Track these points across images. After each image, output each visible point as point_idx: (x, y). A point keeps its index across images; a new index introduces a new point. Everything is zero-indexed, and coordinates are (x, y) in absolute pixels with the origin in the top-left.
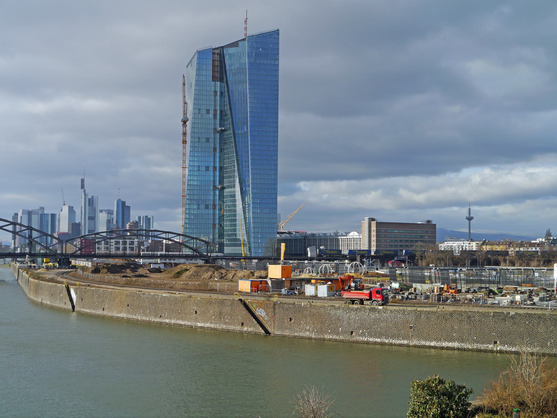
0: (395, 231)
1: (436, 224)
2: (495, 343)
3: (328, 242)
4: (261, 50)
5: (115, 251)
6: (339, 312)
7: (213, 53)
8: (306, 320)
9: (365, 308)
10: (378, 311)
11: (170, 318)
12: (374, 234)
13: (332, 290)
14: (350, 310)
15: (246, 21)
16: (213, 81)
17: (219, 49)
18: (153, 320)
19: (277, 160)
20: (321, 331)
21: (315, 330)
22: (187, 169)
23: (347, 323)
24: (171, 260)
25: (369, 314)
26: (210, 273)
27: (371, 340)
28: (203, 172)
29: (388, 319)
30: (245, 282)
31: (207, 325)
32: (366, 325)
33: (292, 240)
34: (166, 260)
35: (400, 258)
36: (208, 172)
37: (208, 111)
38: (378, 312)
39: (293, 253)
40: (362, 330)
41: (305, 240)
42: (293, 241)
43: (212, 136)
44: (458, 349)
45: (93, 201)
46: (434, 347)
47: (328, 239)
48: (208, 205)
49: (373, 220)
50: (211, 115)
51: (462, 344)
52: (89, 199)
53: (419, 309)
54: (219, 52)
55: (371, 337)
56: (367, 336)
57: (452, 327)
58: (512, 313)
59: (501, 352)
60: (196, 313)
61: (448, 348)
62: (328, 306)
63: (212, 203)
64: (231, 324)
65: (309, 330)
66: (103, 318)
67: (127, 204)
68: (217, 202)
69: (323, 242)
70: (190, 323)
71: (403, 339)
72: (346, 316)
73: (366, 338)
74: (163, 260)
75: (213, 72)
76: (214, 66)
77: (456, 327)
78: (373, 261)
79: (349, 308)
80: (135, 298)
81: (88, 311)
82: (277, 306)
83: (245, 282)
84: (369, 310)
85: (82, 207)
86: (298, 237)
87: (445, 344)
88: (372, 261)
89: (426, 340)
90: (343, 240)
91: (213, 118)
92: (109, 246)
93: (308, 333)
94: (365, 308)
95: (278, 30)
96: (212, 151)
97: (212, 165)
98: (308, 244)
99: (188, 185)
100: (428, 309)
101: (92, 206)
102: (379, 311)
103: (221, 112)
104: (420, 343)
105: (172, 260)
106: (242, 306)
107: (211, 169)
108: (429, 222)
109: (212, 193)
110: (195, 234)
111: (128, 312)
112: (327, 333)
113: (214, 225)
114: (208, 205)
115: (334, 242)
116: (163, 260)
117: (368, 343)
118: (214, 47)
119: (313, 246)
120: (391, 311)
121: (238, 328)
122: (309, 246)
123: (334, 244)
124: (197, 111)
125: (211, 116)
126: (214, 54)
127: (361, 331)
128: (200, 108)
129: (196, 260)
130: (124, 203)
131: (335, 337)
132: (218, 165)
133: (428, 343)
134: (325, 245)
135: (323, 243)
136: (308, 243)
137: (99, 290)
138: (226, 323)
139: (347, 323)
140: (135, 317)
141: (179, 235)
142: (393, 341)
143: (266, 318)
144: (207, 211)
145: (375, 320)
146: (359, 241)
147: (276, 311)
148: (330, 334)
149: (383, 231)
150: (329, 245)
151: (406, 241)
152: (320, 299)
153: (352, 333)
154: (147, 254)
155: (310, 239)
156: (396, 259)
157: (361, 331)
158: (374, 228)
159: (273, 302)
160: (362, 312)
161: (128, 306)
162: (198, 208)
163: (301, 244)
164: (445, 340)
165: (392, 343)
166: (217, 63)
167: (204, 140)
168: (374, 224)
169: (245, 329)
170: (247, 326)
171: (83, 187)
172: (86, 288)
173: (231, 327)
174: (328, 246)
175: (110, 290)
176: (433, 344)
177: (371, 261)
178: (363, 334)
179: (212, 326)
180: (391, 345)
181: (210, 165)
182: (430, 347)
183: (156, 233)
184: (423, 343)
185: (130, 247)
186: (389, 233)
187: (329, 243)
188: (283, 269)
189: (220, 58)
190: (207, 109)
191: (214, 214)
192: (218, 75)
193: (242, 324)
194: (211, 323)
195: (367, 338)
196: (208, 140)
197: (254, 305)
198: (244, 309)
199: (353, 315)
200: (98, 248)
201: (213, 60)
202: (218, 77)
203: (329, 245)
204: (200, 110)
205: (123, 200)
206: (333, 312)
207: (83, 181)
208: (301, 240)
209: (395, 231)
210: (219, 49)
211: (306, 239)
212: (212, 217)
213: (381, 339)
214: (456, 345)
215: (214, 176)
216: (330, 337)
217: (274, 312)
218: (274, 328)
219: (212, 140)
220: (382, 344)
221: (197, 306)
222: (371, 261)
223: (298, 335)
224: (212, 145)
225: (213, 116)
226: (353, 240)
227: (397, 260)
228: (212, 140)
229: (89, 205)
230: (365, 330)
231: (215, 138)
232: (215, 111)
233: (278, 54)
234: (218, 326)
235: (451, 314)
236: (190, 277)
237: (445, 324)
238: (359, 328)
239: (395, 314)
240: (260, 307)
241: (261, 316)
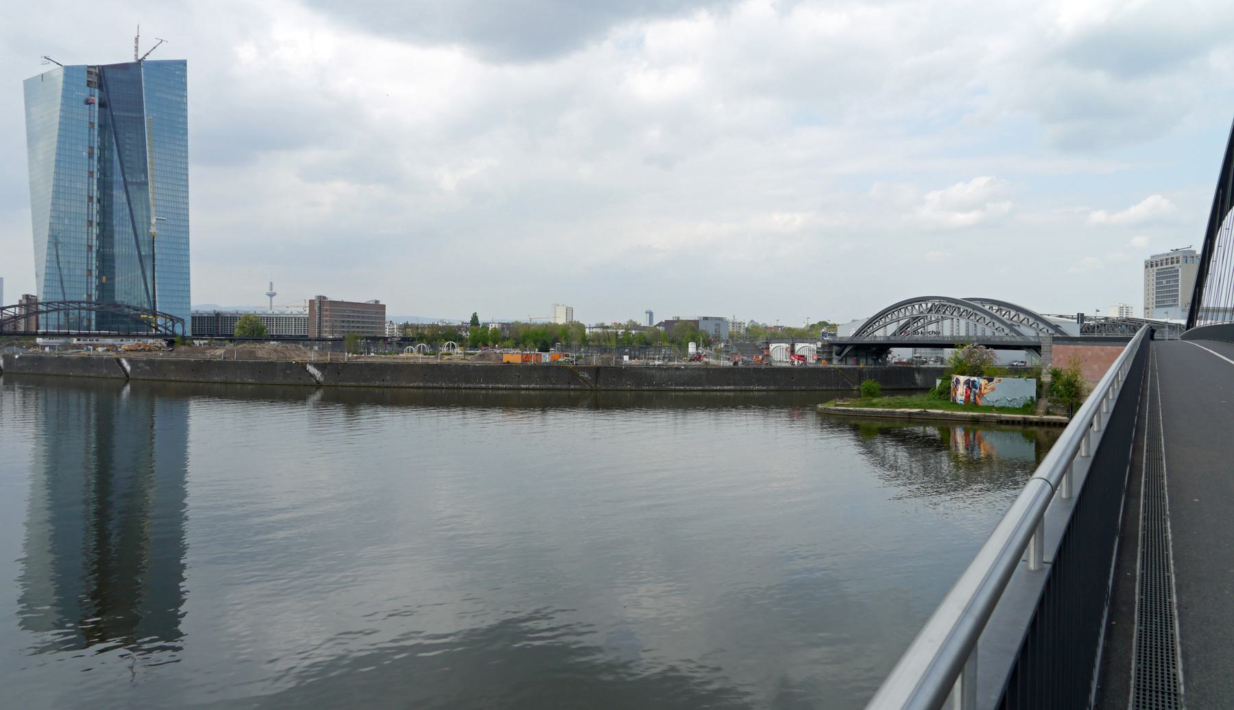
11: (488, 383)
34: (79, 340)
39: (197, 333)
41: (218, 317)
117: (675, 390)
131: (650, 387)
133: (715, 388)
138: (551, 383)
178: (672, 385)
180: (691, 390)
182: (716, 390)
193: (569, 383)
206: (648, 372)
214: (732, 387)
240: (583, 371)
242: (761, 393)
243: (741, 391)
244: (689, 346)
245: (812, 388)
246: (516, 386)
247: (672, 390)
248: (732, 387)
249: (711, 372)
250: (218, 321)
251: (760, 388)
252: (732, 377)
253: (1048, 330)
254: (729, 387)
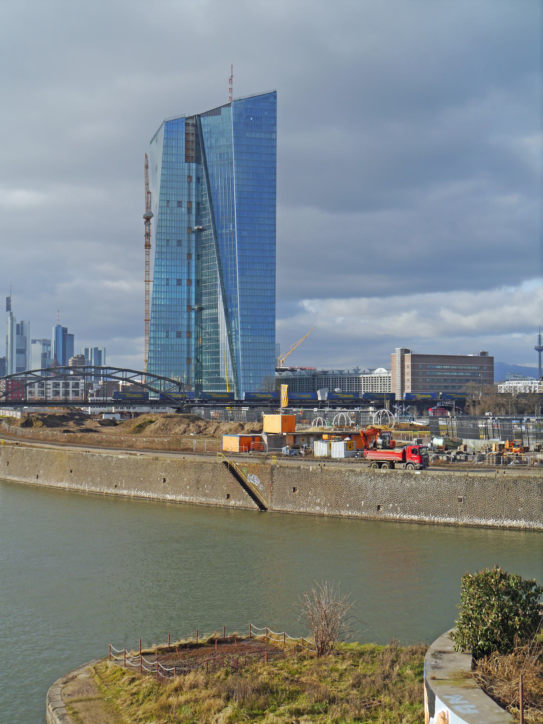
0: (437, 367)
1: (493, 358)
3: (345, 383)
4: (251, 119)
5: (53, 396)
7: (186, 123)
8: (315, 490)
9: (396, 473)
10: (414, 477)
11: (129, 489)
12: (408, 371)
13: (350, 449)
14: (376, 476)
15: (231, 80)
16: (186, 162)
17: (194, 118)
18: (105, 491)
19: (275, 270)
20: (337, 505)
21: (328, 505)
22: (151, 284)
23: (372, 494)
24: (129, 408)
25: (402, 482)
26: (183, 427)
27: (405, 517)
28: (173, 287)
29: (429, 488)
30: (231, 439)
31: (180, 498)
32: (398, 497)
33: (297, 380)
34: (122, 408)
35: (444, 404)
36: (180, 287)
37: (180, 204)
38: (415, 479)
40: (393, 504)
41: (314, 379)
42: (298, 381)
43: (185, 237)
44: (526, 530)
45: (22, 327)
47: (345, 378)
48: (180, 333)
49: (407, 351)
50: (183, 209)
51: (531, 523)
52: (18, 326)
53: (471, 474)
54: (194, 122)
55: (405, 513)
56: (400, 512)
57: (517, 499)
60: (165, 481)
61: (511, 529)
62: (346, 471)
63: (185, 329)
64: (213, 497)
65: (319, 504)
66: (37, 488)
67: (69, 332)
68: (193, 328)
69: (339, 382)
70: (156, 496)
71: (449, 516)
72: (371, 485)
73: (399, 515)
74: (119, 408)
75: (187, 149)
76: (187, 141)
77: (521, 499)
78: (407, 408)
79: (374, 474)
80: (81, 461)
81: (16, 479)
82: (275, 472)
83: (231, 439)
84: (402, 476)
85: (7, 336)
86: (303, 375)
87: (507, 523)
88: (405, 408)
89: (481, 517)
90: (366, 379)
91: (186, 213)
92: (44, 389)
93: (318, 508)
94: (396, 473)
95: (275, 92)
96: (186, 258)
97: (186, 277)
98: (318, 385)
99: (153, 305)
100: (483, 475)
101: (22, 334)
102: (416, 478)
103: (198, 204)
104: (472, 522)
105: (131, 408)
106: (227, 472)
107: (184, 282)
108: (483, 353)
109: (185, 316)
110: (162, 373)
111: (72, 480)
112: (343, 507)
113: (189, 359)
114: (180, 333)
115: (353, 383)
116: (119, 408)
118: (187, 116)
119: (325, 387)
120: (433, 478)
121: (223, 501)
122: (320, 387)
123: (353, 385)
124: (164, 204)
125: (184, 210)
126: (187, 125)
127: (391, 505)
128: (168, 199)
129: (164, 408)
130: (65, 330)
132: (193, 277)
133: (483, 522)
134: (341, 386)
135: (339, 384)
136: (318, 383)
137: (31, 450)
138: (206, 495)
139: (372, 494)
140: (81, 487)
141: (140, 373)
142: (436, 518)
143: (260, 488)
144: (179, 341)
145: (410, 490)
146: (388, 381)
147: (275, 478)
148: (348, 509)
149: (420, 367)
150: (346, 386)
151: (452, 380)
152: (335, 460)
153: (379, 507)
154: (97, 400)
155: (320, 379)
156: (438, 405)
157: (391, 505)
158: (408, 362)
159: (270, 466)
160: (392, 479)
161: (71, 472)
162: (167, 337)
163: (309, 386)
164: (507, 517)
165: (434, 522)
166: (192, 138)
167: (175, 243)
168: (408, 357)
169: (232, 503)
170: (235, 499)
171: (8, 308)
172: (13, 448)
173: (213, 501)
174: (345, 387)
175: (46, 450)
176: (490, 522)
177: (404, 408)
179: (187, 499)
180: (433, 524)
181: (183, 278)
183: (109, 372)
184: (477, 521)
185: (73, 391)
186: (429, 369)
187: (346, 384)
188: (284, 420)
189: (196, 130)
190: (178, 200)
191: (189, 345)
192: (193, 154)
193: (228, 496)
194: (185, 495)
195: (400, 515)
196: (179, 243)
197: (244, 471)
198: (231, 475)
200: (30, 392)
201: (187, 134)
202: (193, 157)
203: (346, 386)
204: (168, 202)
205: (64, 326)
206: (352, 479)
207: (8, 300)
208: (309, 379)
209: (437, 367)
210: (194, 118)
211: (316, 378)
212: (185, 349)
213: (418, 516)
214: (522, 523)
215: (189, 292)
216: (348, 513)
217: (271, 479)
218: (272, 502)
219: (185, 244)
220: (421, 523)
221: (166, 471)
222: (404, 408)
223: (305, 510)
224: (185, 251)
225: (186, 210)
226: (379, 380)
227: (441, 407)
228: (185, 244)
229: (18, 333)
230: (396, 504)
231: (189, 241)
232: (190, 203)
233: (275, 125)
234: (194, 499)
235: (515, 481)
236: (156, 432)
237: (507, 495)
238: (389, 501)
239: (438, 481)
241: (253, 485)
246: (160, 496)
250: (314, 382)
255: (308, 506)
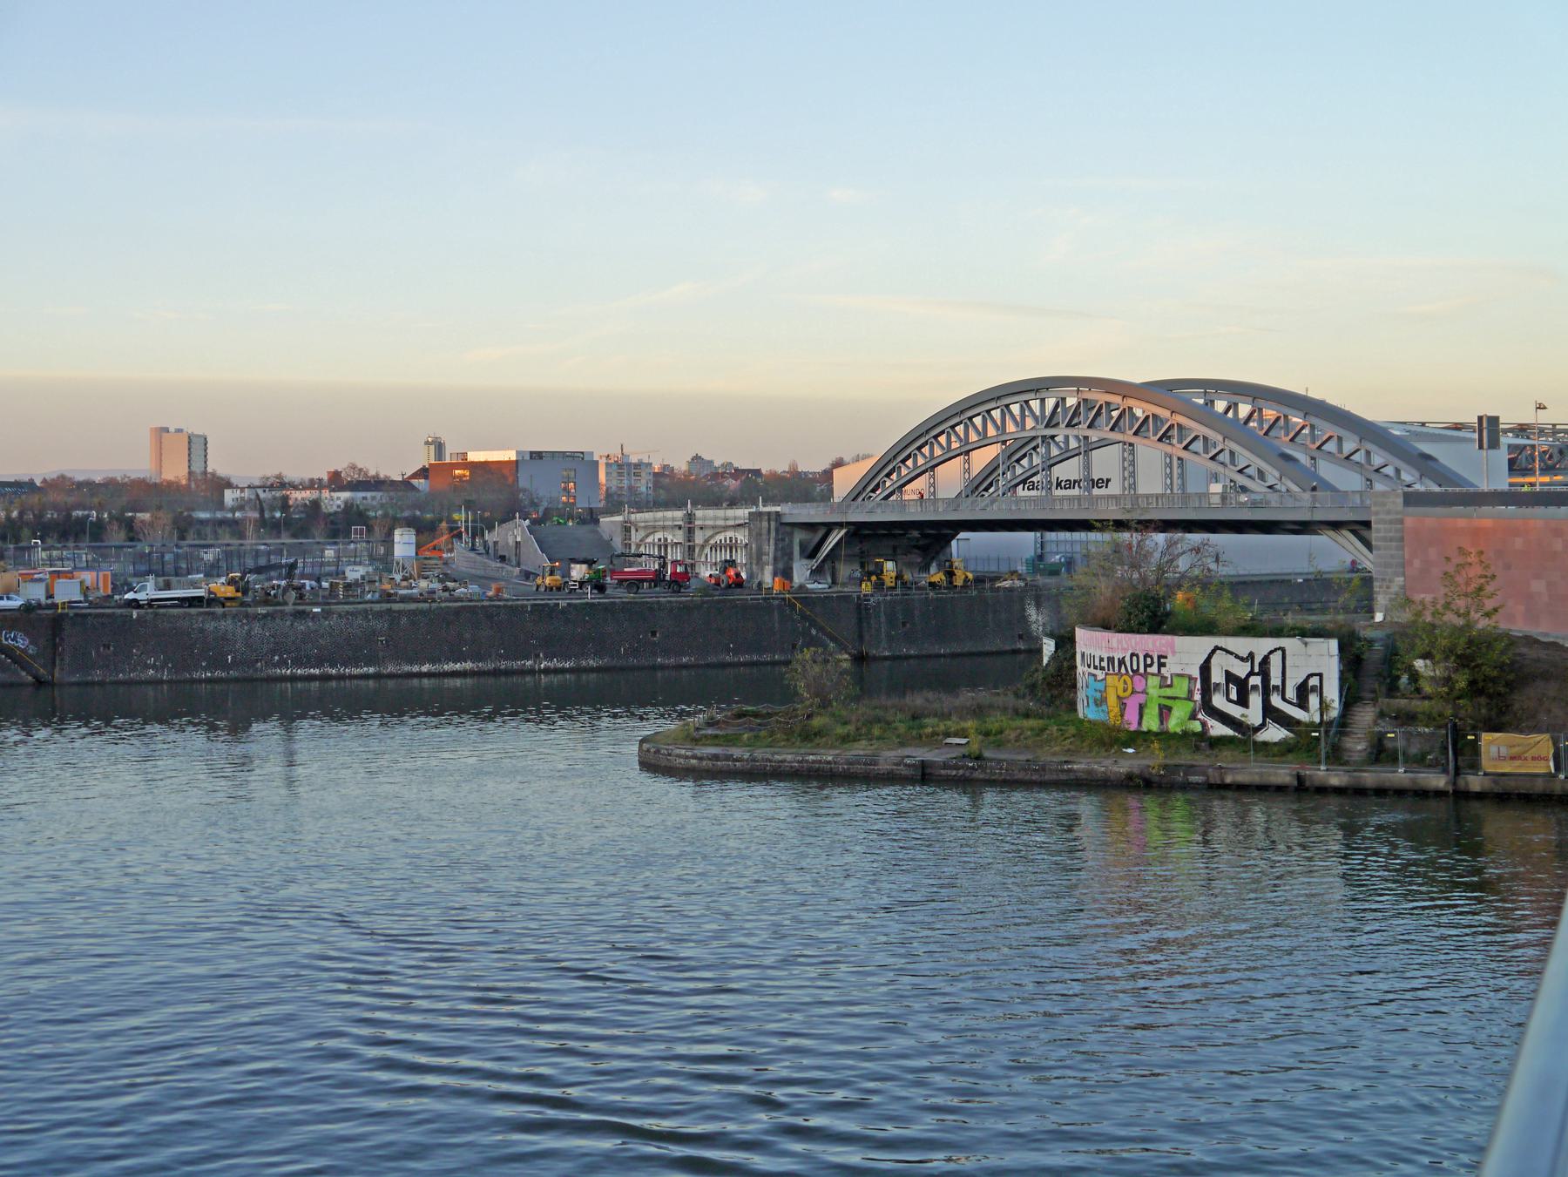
2: (537, 656)
6: (226, 625)
38: (313, 618)
46: (429, 675)
51: (480, 665)
58: (563, 603)
59: (547, 671)
65: (154, 667)
71: (367, 665)
73: (289, 671)
79: (247, 616)
89: (411, 662)
112: (197, 667)
117: (294, 679)
120: (340, 616)
133: (416, 669)
143: (30, 651)
148: (205, 669)
157: (276, 658)
160: (278, 621)
164: (448, 660)
165: (344, 674)
176: (425, 668)
182: (420, 675)
184: (407, 668)
199: (257, 629)
206: (210, 626)
214: (468, 665)
220: (326, 678)
238: (274, 652)
240: (11, 629)
241: (18, 648)
242: (555, 679)
243: (496, 673)
244: (397, 538)
245: (712, 659)
247: (284, 679)
248: (468, 665)
249: (404, 620)
251: (555, 663)
252: (467, 636)
253: (1398, 471)
254: (458, 666)
255: (131, 671)
